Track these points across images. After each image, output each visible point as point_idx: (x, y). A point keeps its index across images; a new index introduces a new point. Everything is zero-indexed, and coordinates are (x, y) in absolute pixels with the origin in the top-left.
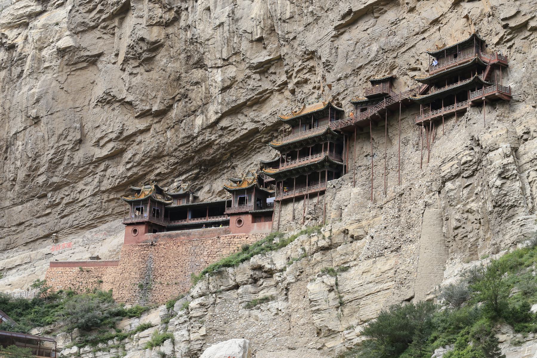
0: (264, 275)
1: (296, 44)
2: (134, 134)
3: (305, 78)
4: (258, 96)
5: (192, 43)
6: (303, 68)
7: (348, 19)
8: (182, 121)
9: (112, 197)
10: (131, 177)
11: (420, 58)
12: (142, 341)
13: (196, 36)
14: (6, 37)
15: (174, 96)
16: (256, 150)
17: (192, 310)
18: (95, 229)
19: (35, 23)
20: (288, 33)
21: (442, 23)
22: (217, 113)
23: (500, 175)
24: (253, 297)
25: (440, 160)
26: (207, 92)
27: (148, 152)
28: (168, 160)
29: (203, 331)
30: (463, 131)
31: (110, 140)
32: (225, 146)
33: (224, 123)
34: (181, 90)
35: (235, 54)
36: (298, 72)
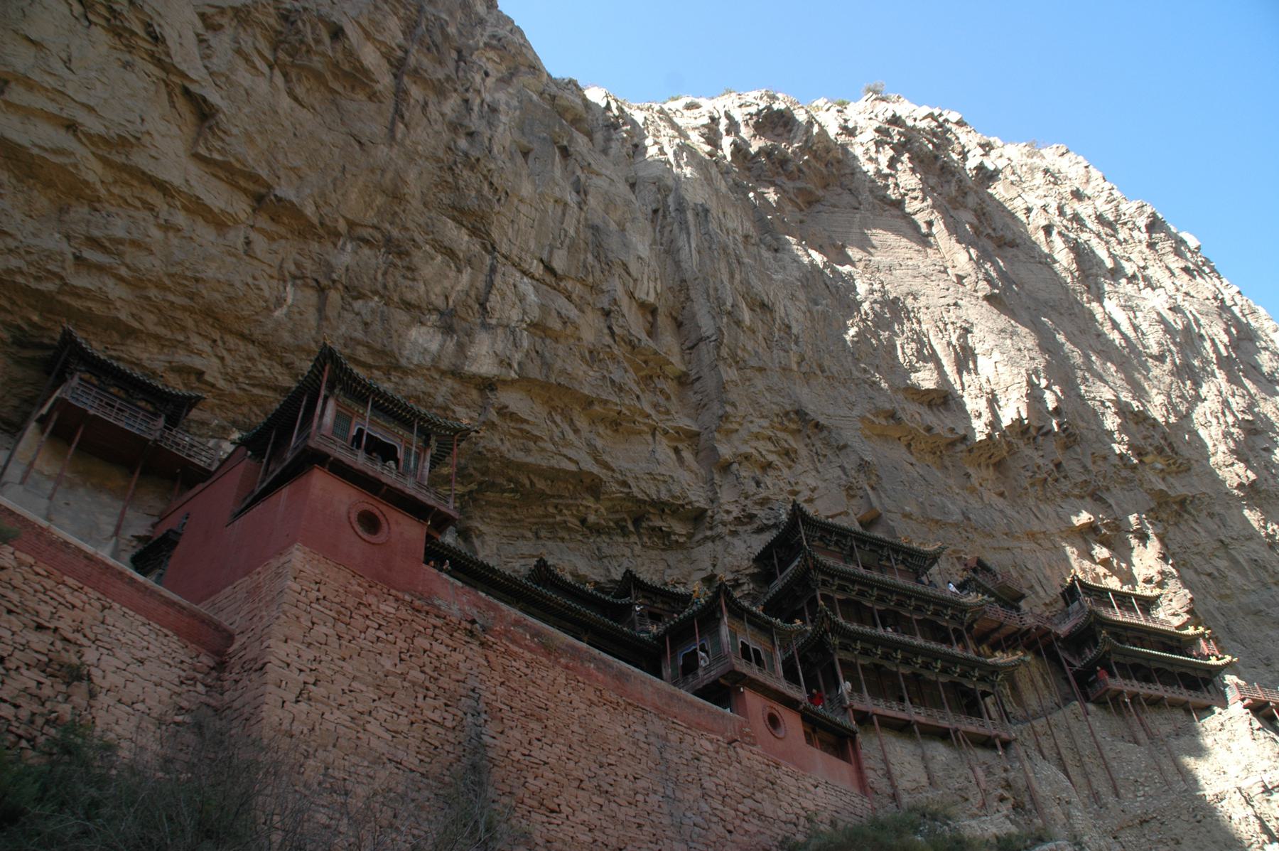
1: (760, 383)
3: (771, 457)
4: (625, 411)
6: (770, 439)
8: (361, 296)
10: (80, 297)
11: (1028, 574)
13: (492, 166)
15: (357, 221)
16: (555, 530)
20: (744, 349)
21: (1040, 545)
22: (505, 363)
26: (473, 294)
27: (197, 280)
28: (251, 359)
31: (71, 127)
32: (488, 460)
33: (513, 399)
34: (388, 226)
35: (582, 281)
36: (757, 437)
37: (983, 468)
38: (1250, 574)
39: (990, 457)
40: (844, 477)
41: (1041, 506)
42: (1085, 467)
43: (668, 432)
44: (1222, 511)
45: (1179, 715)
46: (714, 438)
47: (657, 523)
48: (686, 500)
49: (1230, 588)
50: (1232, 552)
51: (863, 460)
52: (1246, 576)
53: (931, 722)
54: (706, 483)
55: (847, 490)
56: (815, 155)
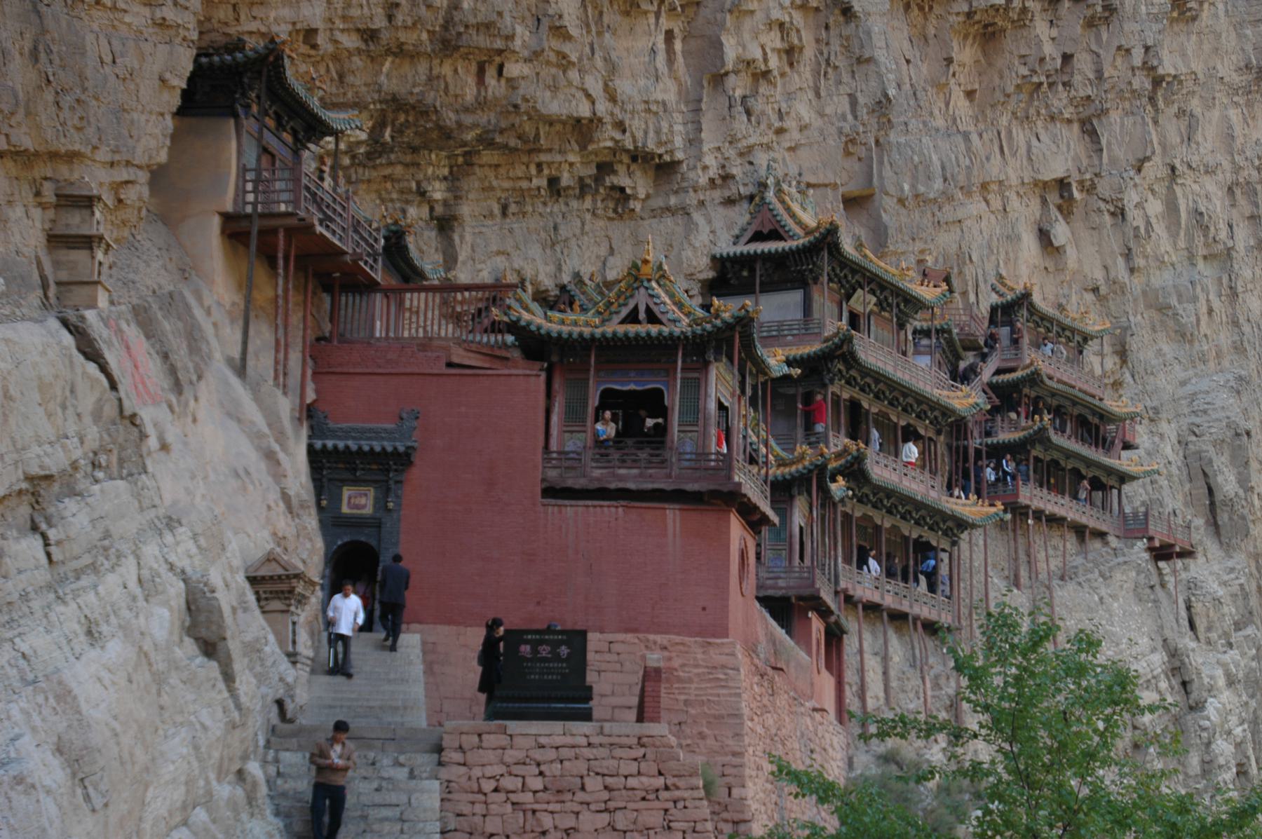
11: (969, 271)
21: (987, 202)
37: (970, 40)
38: (1182, 234)
39: (986, 26)
40: (850, 117)
41: (1014, 131)
42: (1099, 74)
43: (675, 9)
44: (1198, 111)
45: (1071, 542)
46: (722, 26)
47: (622, 180)
48: (669, 147)
49: (1146, 257)
50: (1178, 190)
51: (886, 96)
52: (1174, 236)
53: (898, 607)
54: (687, 103)
55: (846, 143)
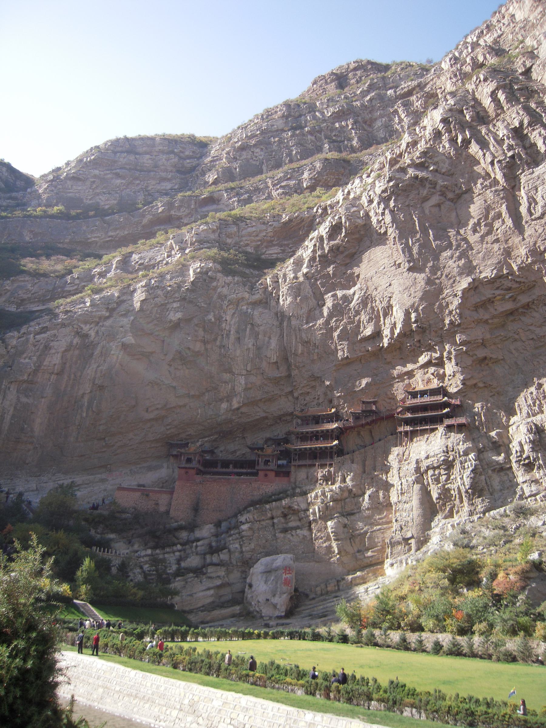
0: (291, 512)
2: (175, 407)
5: (225, 357)
7: (345, 362)
9: (153, 445)
12: (199, 548)
14: (82, 329)
17: (243, 531)
18: (138, 466)
19: (105, 323)
22: (239, 403)
23: (472, 471)
24: (284, 525)
25: (423, 455)
29: (252, 546)
30: (439, 440)
33: (244, 410)
36: (303, 387)
47: (284, 418)
56: (352, 233)
